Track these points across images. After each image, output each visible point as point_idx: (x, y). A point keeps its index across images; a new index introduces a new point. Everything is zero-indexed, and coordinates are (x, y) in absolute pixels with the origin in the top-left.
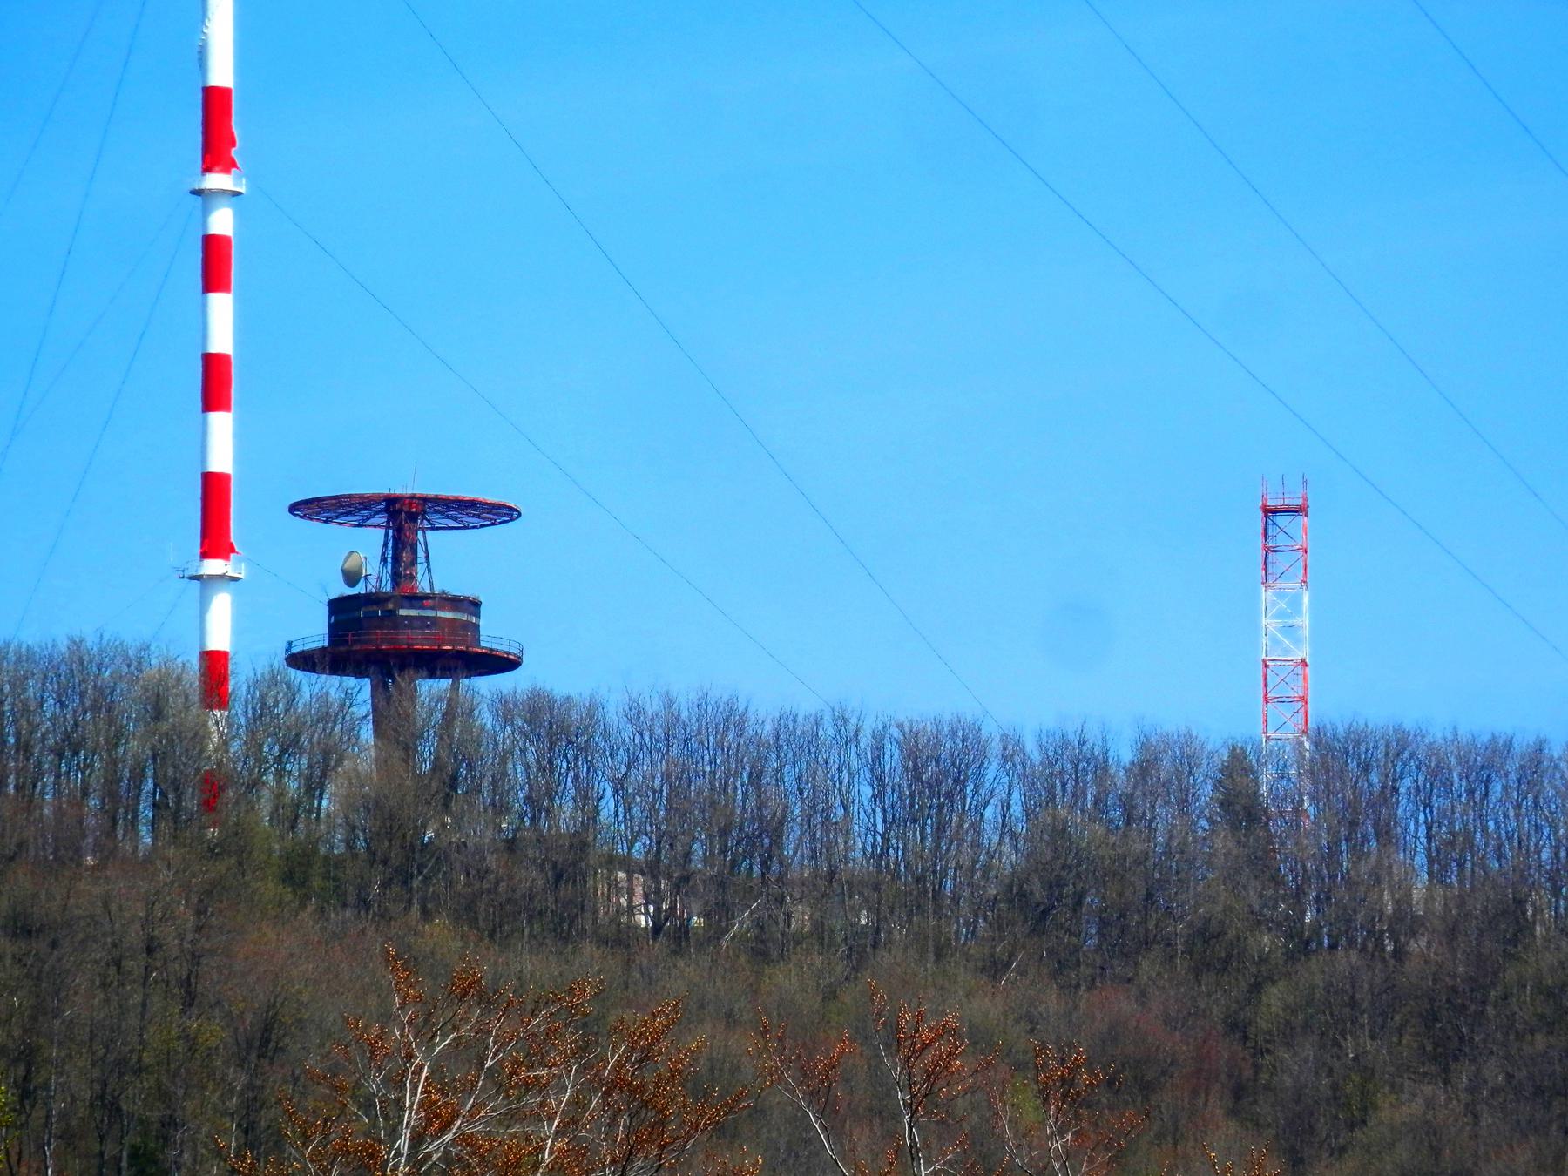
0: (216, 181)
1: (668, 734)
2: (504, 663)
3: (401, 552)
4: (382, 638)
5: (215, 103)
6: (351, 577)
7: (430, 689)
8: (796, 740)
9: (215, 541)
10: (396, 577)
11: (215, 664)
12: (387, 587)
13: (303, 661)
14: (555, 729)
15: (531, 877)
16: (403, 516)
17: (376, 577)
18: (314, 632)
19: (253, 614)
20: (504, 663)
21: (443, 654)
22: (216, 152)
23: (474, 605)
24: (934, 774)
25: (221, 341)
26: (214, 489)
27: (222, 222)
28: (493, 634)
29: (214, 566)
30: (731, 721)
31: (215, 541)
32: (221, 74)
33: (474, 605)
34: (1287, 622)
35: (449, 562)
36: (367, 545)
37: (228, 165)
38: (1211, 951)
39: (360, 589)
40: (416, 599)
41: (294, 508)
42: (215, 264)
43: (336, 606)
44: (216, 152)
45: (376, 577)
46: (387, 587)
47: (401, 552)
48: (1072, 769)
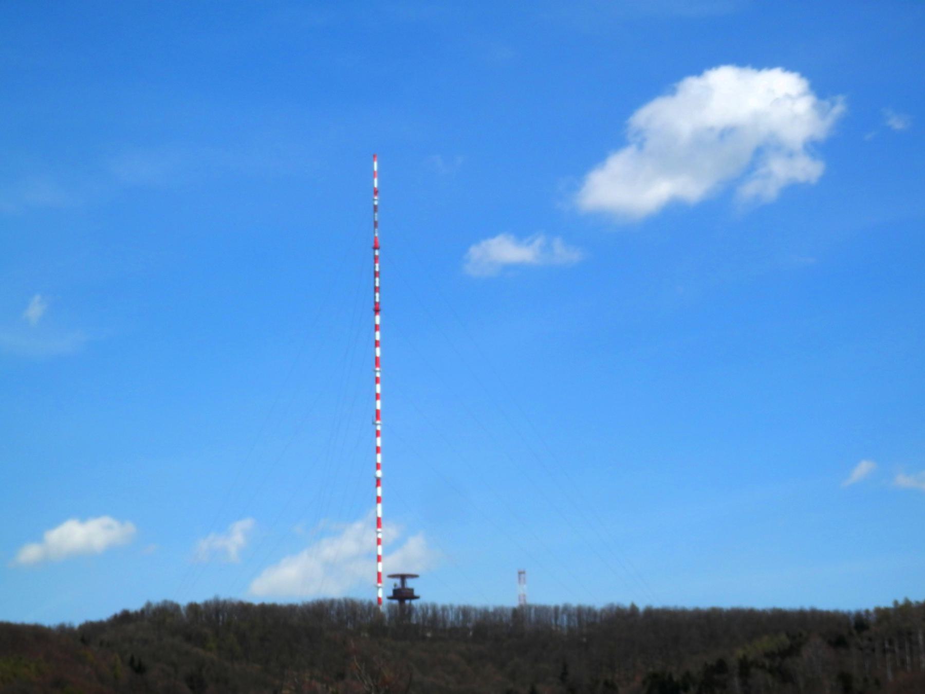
1: (424, 609)
2: (417, 598)
3: (403, 582)
4: (402, 594)
5: (379, 520)
7: (407, 602)
8: (444, 609)
9: (379, 580)
11: (379, 600)
14: (411, 609)
16: (403, 577)
18: (391, 593)
19: (383, 592)
20: (417, 598)
26: (379, 574)
28: (416, 593)
29: (379, 585)
30: (434, 607)
31: (379, 580)
32: (380, 515)
34: (523, 589)
35: (410, 583)
36: (398, 581)
47: (403, 582)
48: (485, 614)
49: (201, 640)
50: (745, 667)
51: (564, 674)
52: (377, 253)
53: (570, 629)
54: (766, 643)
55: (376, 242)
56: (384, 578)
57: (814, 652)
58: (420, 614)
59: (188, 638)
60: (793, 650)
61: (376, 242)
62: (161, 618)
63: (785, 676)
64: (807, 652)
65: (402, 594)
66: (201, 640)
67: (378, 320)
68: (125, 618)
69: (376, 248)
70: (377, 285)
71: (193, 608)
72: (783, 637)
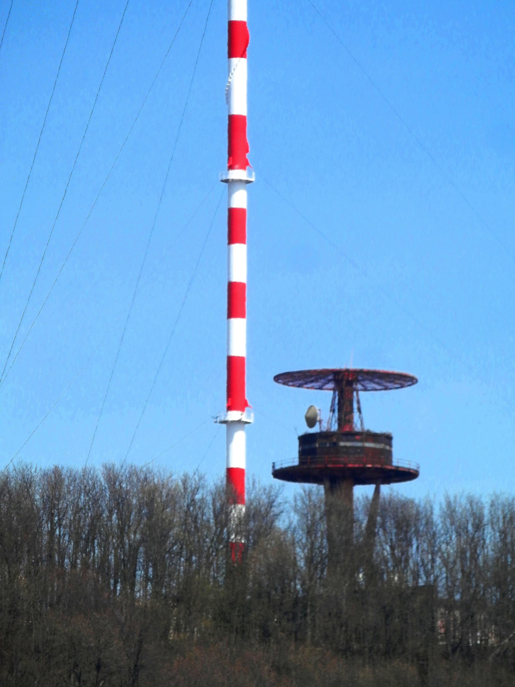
2: (407, 475)
3: (344, 407)
4: (338, 459)
5: (235, 125)
6: (311, 421)
7: (362, 492)
9: (235, 398)
10: (340, 421)
12: (335, 428)
13: (283, 474)
14: (406, 522)
16: (345, 383)
17: (328, 421)
18: (291, 457)
19: (256, 446)
20: (407, 475)
21: (364, 470)
22: (236, 155)
23: (388, 439)
25: (239, 274)
26: (234, 366)
27: (240, 200)
28: (401, 457)
31: (235, 398)
32: (239, 107)
33: (388, 439)
35: (374, 411)
36: (322, 400)
37: (244, 165)
39: (316, 429)
40: (352, 435)
41: (277, 378)
42: (235, 227)
43: (305, 440)
44: (236, 155)
46: (335, 428)
47: (344, 407)
56: (257, 384)
65: (338, 459)
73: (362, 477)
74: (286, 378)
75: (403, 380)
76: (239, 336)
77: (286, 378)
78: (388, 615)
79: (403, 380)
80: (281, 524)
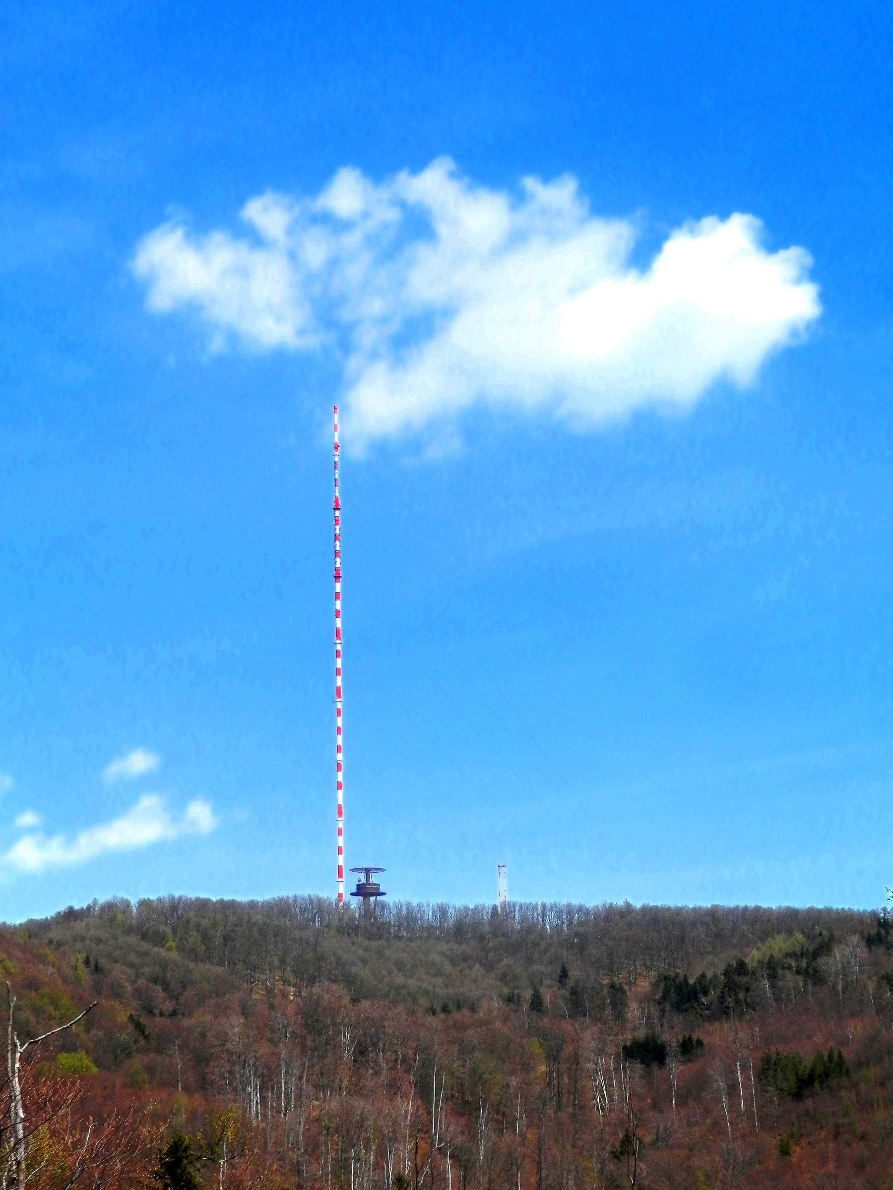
0: (340, 819)
1: (399, 907)
2: (383, 894)
3: (368, 877)
5: (340, 807)
7: (372, 899)
9: (341, 876)
11: (340, 895)
13: (352, 894)
14: (383, 906)
15: (375, 930)
16: (367, 871)
17: (364, 881)
20: (383, 894)
24: (442, 911)
26: (340, 868)
28: (382, 890)
31: (341, 876)
35: (374, 878)
36: (362, 876)
38: (482, 938)
45: (364, 881)
47: (368, 877)
49: (159, 939)
50: (772, 967)
51: (564, 975)
52: (337, 513)
53: (558, 930)
54: (779, 945)
55: (337, 502)
57: (848, 953)
58: (394, 911)
59: (144, 937)
60: (824, 947)
61: (337, 502)
62: (112, 914)
63: (815, 976)
64: (838, 953)
66: (159, 939)
67: (338, 587)
68: (70, 915)
69: (337, 508)
70: (338, 548)
71: (145, 904)
72: (800, 937)
73: (373, 895)
74: (353, 870)
75: (382, 870)
76: (341, 860)
77: (353, 870)
78: (379, 929)
79: (382, 870)
80: (352, 907)
